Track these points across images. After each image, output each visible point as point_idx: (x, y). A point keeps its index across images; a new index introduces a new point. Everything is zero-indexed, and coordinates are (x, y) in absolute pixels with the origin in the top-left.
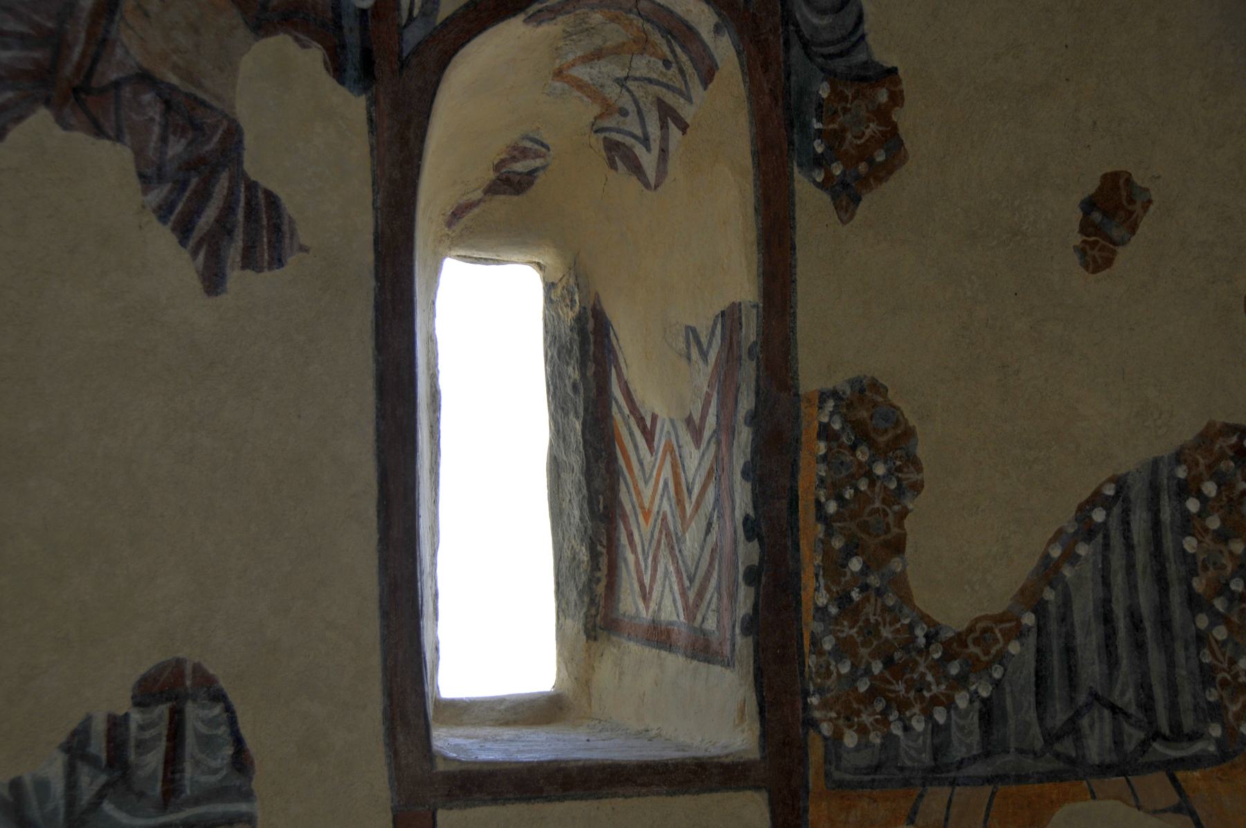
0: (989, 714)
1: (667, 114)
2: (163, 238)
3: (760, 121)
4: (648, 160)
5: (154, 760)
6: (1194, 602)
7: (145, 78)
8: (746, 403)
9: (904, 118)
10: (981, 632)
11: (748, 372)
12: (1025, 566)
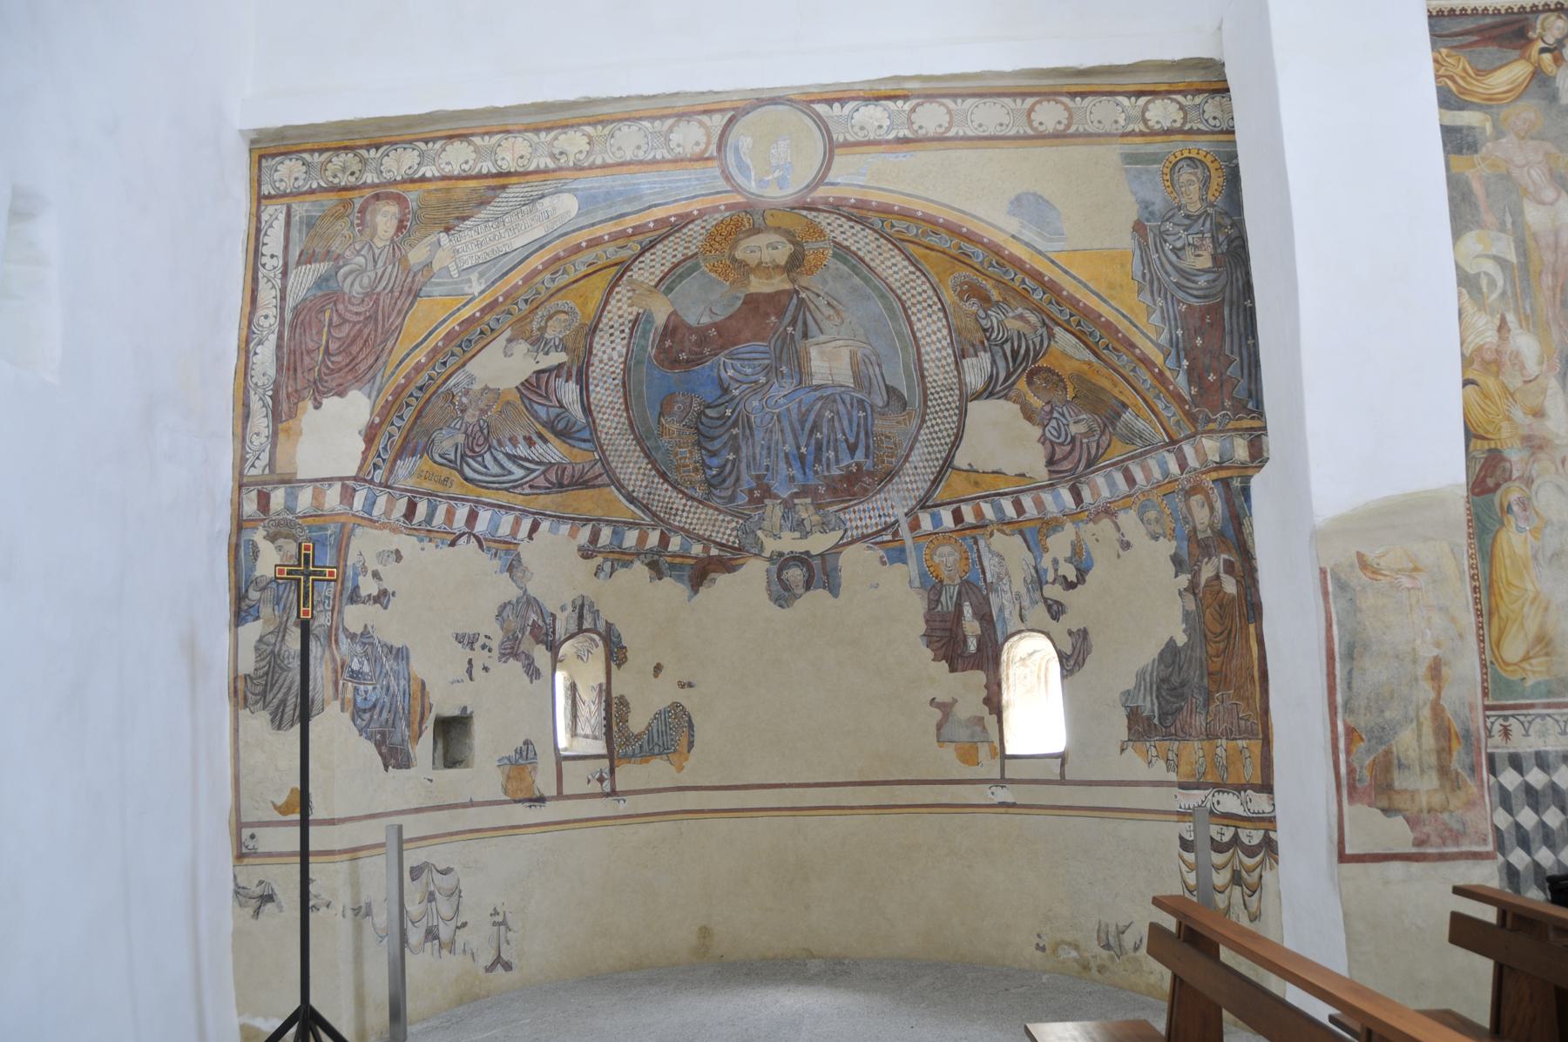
0: (641, 746)
1: (588, 651)
2: (525, 675)
3: (606, 655)
4: (585, 658)
5: (525, 754)
6: (670, 729)
7: (523, 652)
8: (604, 698)
9: (628, 654)
10: (640, 734)
11: (604, 694)
12: (646, 724)
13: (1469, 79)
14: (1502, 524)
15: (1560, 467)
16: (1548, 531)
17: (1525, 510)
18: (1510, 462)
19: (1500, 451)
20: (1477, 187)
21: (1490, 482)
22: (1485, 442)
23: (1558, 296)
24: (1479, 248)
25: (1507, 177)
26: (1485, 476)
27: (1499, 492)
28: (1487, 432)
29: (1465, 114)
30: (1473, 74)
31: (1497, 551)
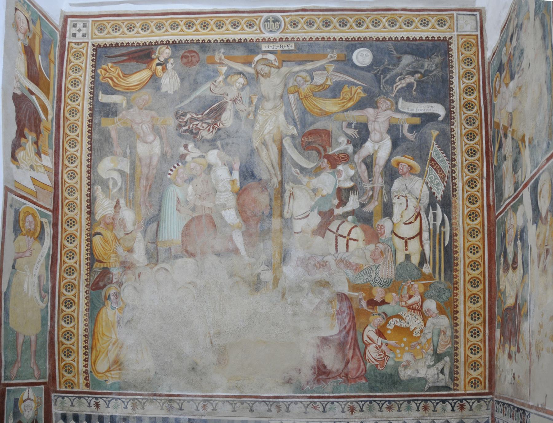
13: (119, 79)
14: (104, 305)
15: (137, 278)
16: (126, 309)
17: (117, 299)
18: (112, 274)
19: (108, 269)
20: (113, 134)
21: (101, 284)
22: (102, 264)
23: (148, 191)
24: (112, 165)
25: (131, 129)
26: (99, 281)
27: (105, 289)
28: (104, 259)
29: (114, 97)
30: (121, 76)
31: (99, 319)
